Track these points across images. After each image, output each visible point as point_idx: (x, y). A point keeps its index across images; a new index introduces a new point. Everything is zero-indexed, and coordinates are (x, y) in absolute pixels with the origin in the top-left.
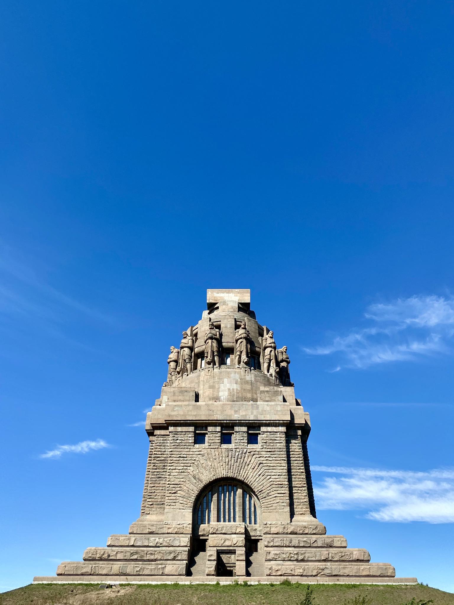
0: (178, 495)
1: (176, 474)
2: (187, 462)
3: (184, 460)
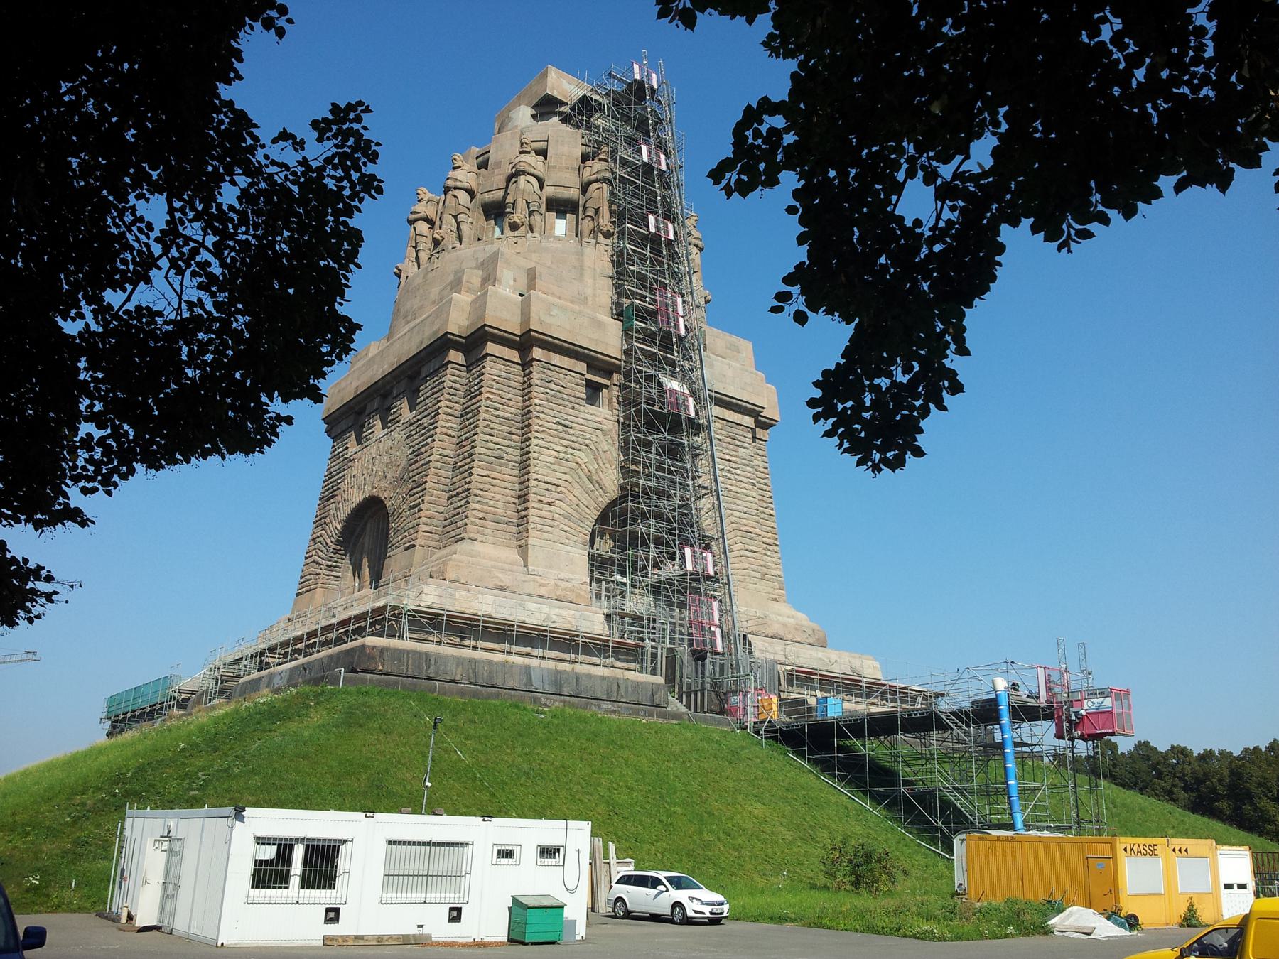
0: (558, 510)
1: (552, 460)
2: (574, 438)
3: (566, 433)
